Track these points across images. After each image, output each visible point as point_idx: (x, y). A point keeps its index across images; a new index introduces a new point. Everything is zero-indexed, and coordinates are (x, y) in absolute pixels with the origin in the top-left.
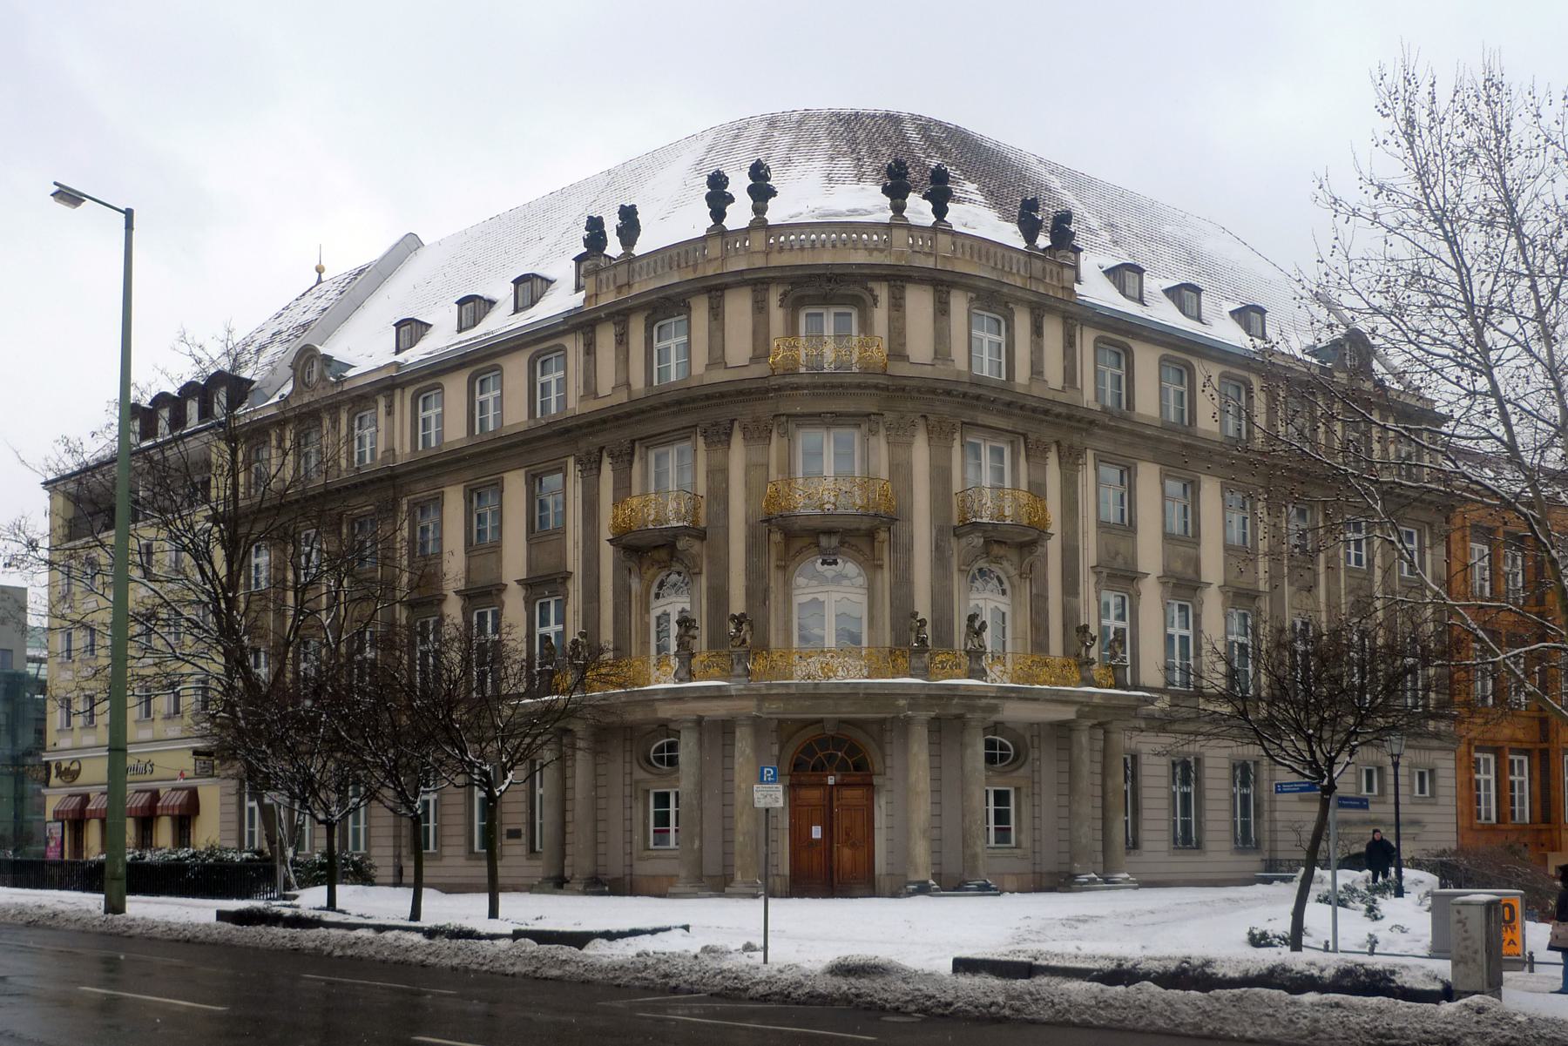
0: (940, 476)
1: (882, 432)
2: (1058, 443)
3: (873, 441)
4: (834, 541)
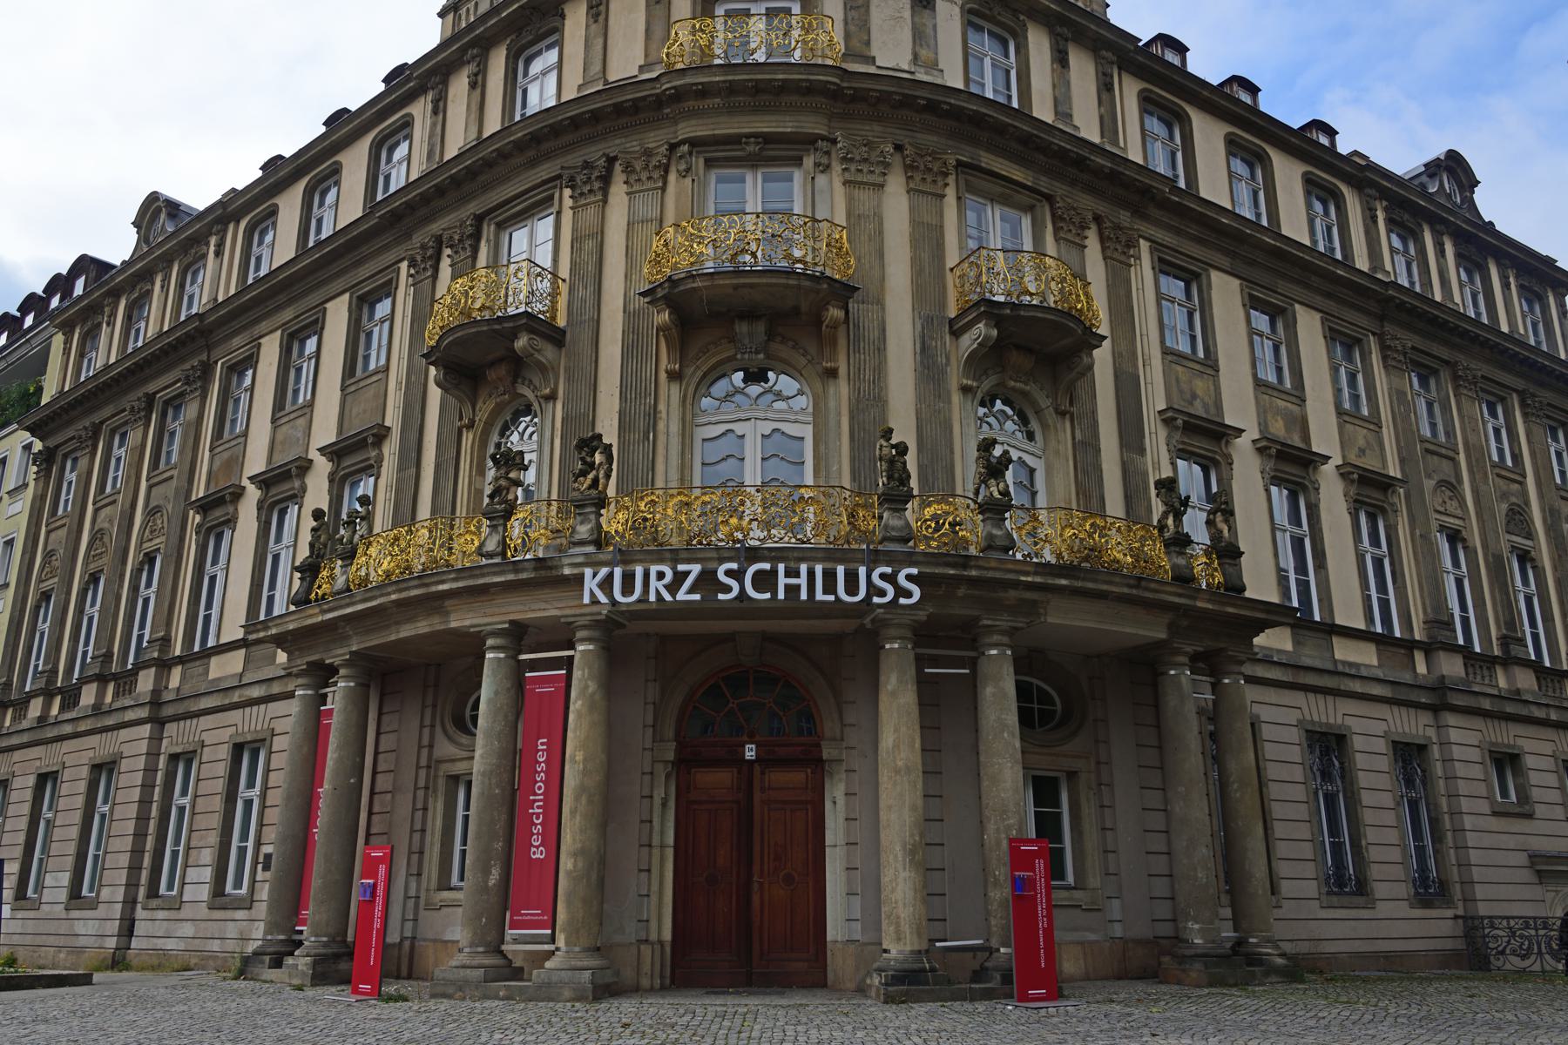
0: (927, 238)
1: (837, 168)
2: (1097, 219)
3: (821, 180)
4: (760, 328)
